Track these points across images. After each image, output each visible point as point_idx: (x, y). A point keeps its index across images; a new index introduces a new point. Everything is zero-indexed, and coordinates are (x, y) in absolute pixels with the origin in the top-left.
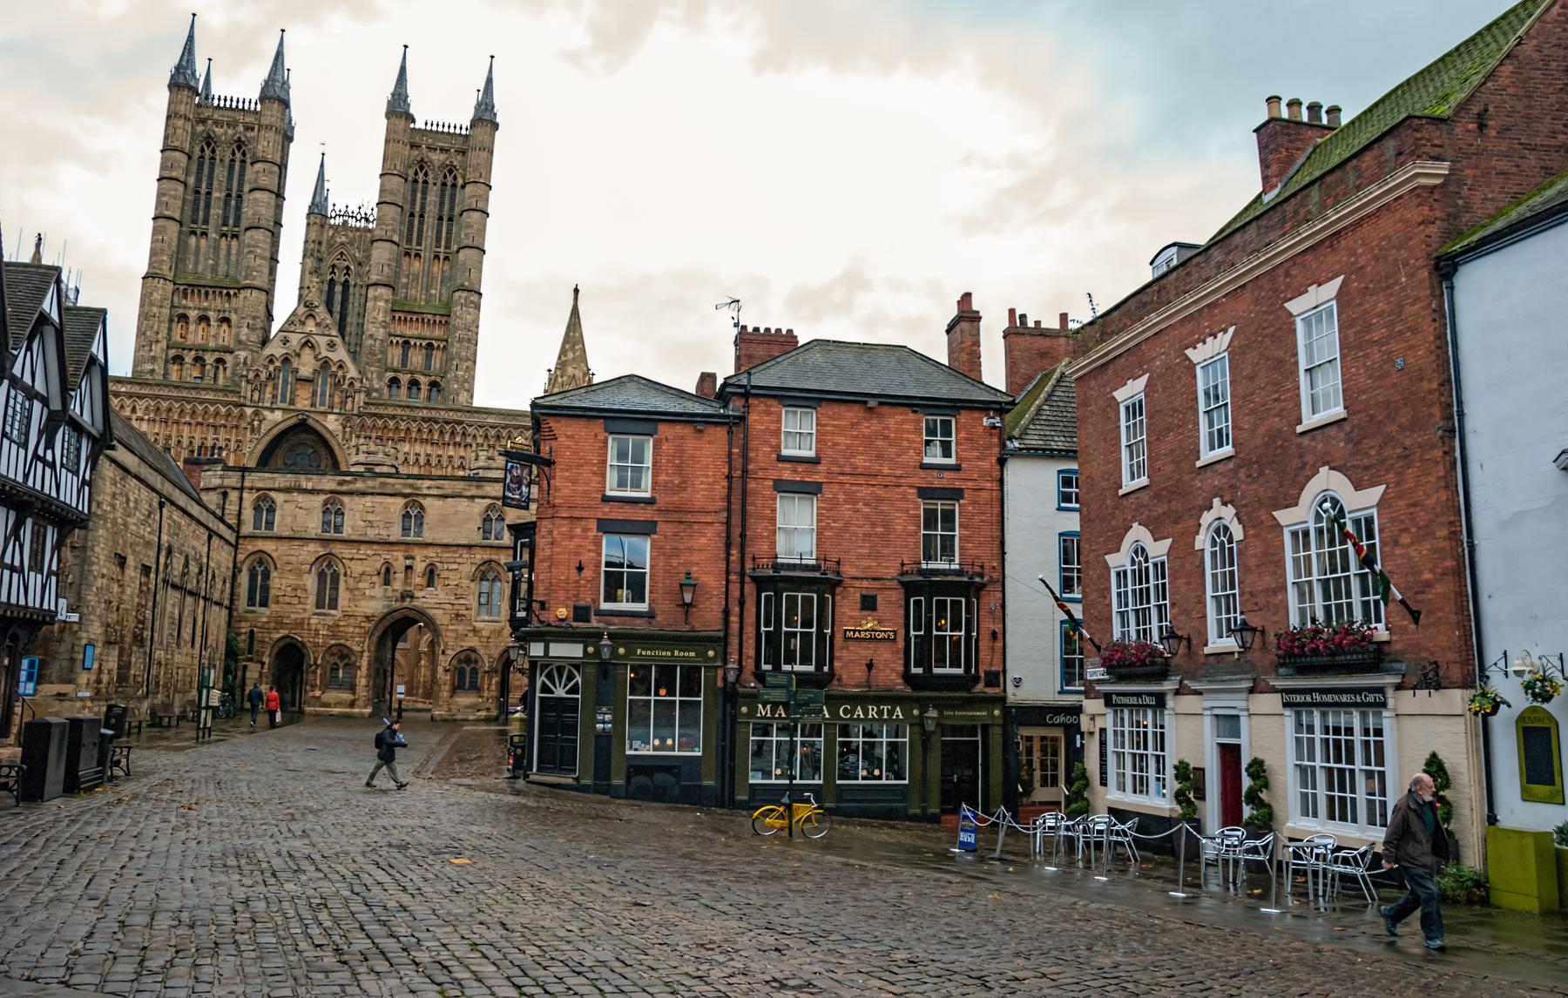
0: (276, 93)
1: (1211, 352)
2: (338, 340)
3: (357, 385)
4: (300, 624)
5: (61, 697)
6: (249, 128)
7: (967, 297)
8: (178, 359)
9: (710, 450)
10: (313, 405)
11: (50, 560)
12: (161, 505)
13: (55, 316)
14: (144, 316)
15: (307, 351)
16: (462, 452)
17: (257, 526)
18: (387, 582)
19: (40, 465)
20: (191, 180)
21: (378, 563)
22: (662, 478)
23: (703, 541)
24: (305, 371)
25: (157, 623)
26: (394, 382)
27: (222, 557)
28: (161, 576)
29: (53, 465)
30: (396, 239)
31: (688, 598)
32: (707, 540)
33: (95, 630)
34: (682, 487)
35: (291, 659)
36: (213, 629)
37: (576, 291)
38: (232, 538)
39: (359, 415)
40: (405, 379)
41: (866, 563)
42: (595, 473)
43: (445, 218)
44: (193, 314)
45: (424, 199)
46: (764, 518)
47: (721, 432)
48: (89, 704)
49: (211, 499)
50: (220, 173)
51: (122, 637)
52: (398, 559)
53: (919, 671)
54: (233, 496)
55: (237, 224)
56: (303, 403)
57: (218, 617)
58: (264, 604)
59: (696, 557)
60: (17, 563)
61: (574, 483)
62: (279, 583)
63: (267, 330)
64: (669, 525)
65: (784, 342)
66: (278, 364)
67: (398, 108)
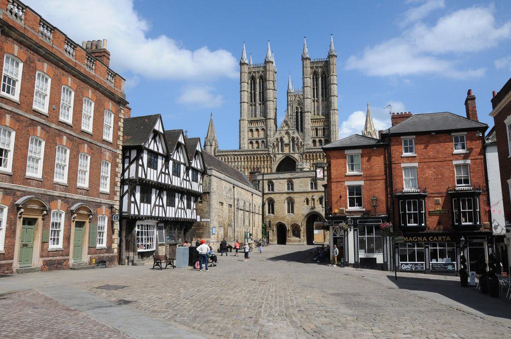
2: (296, 131)
3: (303, 143)
4: (283, 218)
6: (263, 72)
8: (251, 143)
10: (290, 151)
12: (234, 187)
13: (183, 142)
17: (269, 190)
18: (308, 204)
20: (249, 90)
22: (364, 166)
23: (379, 185)
25: (236, 220)
26: (314, 142)
27: (258, 200)
28: (236, 208)
29: (189, 181)
30: (309, 97)
32: (380, 185)
34: (371, 168)
36: (256, 221)
38: (261, 194)
39: (304, 153)
40: (317, 140)
42: (343, 167)
43: (324, 88)
45: (317, 83)
46: (399, 176)
48: (215, 243)
51: (224, 225)
52: (310, 196)
53: (457, 224)
54: (261, 182)
56: (286, 150)
57: (258, 219)
59: (377, 191)
60: (183, 207)
61: (337, 170)
62: (275, 206)
64: (368, 181)
66: (279, 140)
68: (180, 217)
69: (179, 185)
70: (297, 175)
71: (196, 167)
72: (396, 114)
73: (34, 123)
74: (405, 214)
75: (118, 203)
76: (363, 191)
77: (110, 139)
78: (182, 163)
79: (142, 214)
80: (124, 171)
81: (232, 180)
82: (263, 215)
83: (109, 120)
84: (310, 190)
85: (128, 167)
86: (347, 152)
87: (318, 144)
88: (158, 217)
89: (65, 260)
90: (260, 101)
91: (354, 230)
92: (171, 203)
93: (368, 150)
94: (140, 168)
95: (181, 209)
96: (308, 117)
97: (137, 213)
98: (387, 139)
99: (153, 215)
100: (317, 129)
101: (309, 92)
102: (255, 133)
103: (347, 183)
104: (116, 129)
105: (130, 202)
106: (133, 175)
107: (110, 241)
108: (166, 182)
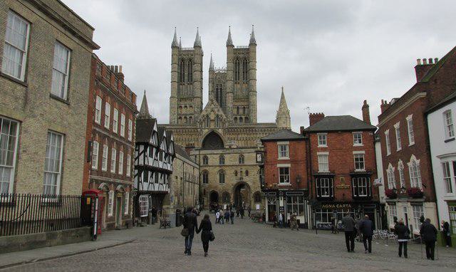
0: (197, 46)
1: (397, 126)
5: (168, 208)
7: (365, 101)
8: (180, 118)
9: (301, 147)
11: (167, 181)
14: (171, 108)
16: (255, 135)
21: (233, 171)
24: (212, 118)
26: (236, 118)
27: (197, 173)
31: (298, 181)
32: (302, 167)
33: (173, 194)
35: (214, 196)
37: (282, 88)
44: (183, 106)
47: (304, 142)
49: (193, 158)
50: (186, 68)
52: (239, 169)
55: (192, 79)
56: (212, 127)
57: (197, 187)
58: (207, 182)
62: (210, 177)
63: (201, 108)
65: (320, 116)
67: (229, 45)
70: (228, 151)
73: (105, 136)
74: (319, 189)
81: (182, 158)
82: (200, 185)
84: (237, 163)
85: (138, 158)
86: (278, 143)
87: (238, 121)
92: (157, 182)
93: (294, 142)
98: (307, 135)
100: (238, 108)
103: (279, 165)
105: (139, 182)
106: (141, 163)
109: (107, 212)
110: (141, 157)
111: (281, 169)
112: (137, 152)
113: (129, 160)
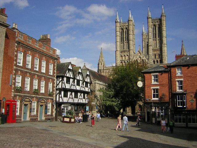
15: (140, 58)
19: (82, 88)
20: (120, 35)
26: (154, 61)
30: (151, 38)
37: (182, 41)
40: (156, 60)
41: (191, 90)
68: (80, 102)
69: (79, 89)
71: (87, 81)
72: (177, 55)
73: (27, 72)
75: (55, 98)
76: (159, 91)
77: (52, 74)
78: (81, 80)
79: (64, 101)
80: (57, 85)
83: (51, 67)
85: (59, 84)
87: (156, 62)
88: (71, 103)
89: (37, 118)
90: (126, 41)
91: (155, 108)
94: (63, 84)
95: (81, 99)
96: (151, 48)
97: (62, 101)
99: (69, 102)
101: (151, 35)
102: (124, 58)
103: (152, 88)
104: (54, 69)
105: (59, 97)
106: (60, 87)
107: (52, 112)
108: (74, 89)
109: (30, 112)
110: (61, 83)
111: (154, 89)
112: (58, 81)
113: (50, 85)
